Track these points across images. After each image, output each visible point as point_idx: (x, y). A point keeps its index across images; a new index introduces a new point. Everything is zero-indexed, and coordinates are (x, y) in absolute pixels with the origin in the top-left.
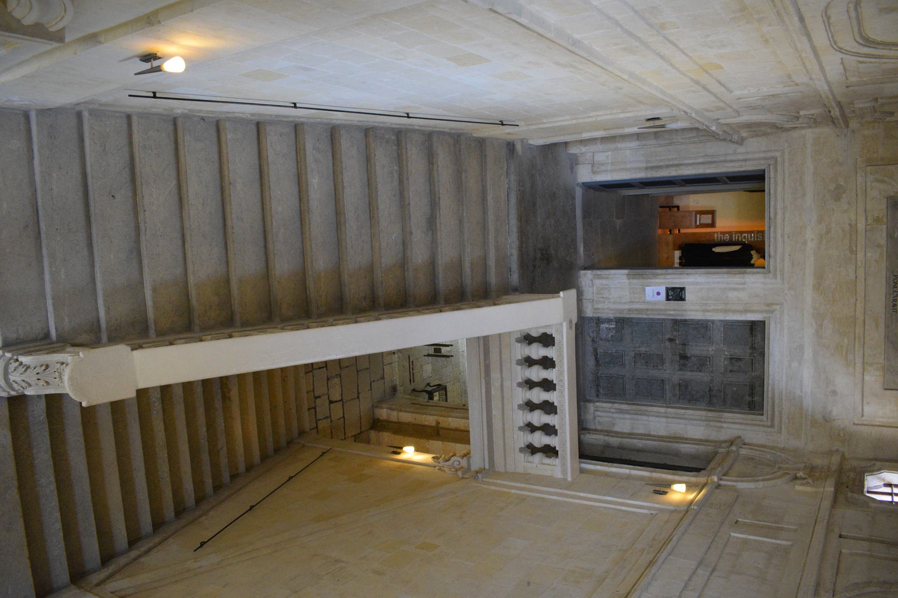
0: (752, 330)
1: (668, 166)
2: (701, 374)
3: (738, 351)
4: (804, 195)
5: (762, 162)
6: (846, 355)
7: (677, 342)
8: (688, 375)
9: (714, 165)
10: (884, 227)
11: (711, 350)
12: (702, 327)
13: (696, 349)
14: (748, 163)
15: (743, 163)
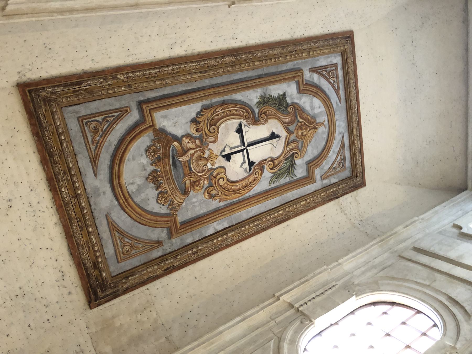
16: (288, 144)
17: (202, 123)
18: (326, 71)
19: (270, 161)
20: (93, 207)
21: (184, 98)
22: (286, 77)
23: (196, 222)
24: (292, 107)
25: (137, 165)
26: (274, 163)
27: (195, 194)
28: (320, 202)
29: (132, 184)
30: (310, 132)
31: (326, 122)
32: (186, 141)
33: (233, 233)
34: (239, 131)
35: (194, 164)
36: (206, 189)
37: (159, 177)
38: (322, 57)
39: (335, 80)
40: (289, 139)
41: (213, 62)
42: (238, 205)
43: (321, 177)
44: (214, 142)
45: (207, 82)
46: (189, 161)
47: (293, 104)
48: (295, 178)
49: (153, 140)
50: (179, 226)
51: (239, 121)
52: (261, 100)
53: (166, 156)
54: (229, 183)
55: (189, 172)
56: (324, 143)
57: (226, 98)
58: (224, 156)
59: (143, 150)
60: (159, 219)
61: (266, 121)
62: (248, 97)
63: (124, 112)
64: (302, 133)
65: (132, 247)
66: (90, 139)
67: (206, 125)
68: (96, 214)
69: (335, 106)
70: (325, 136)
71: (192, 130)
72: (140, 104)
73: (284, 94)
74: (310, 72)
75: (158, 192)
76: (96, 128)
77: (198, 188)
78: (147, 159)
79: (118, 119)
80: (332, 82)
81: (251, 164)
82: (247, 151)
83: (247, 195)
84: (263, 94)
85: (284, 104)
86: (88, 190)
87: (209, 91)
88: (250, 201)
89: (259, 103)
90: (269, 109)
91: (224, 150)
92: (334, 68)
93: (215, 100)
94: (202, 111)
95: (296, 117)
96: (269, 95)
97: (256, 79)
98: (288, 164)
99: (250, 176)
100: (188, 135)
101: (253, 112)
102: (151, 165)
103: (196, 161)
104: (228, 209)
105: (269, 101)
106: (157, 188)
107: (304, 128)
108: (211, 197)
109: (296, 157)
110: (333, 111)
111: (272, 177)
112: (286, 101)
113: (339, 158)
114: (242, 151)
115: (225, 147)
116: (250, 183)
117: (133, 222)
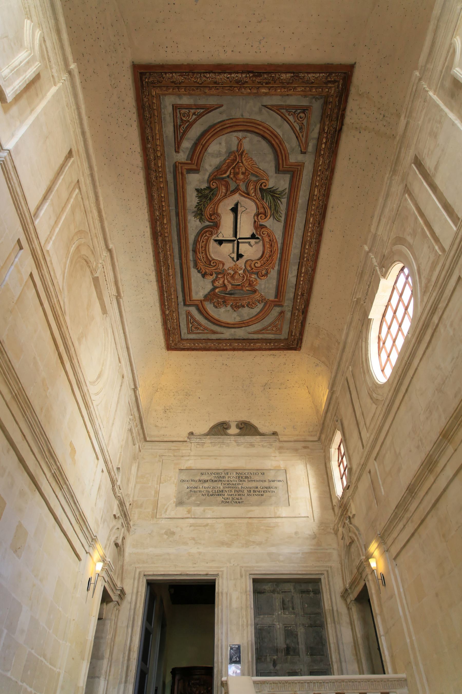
0: (260, 593)
1: (129, 659)
2: (299, 634)
3: (277, 603)
4: (168, 554)
5: (141, 580)
6: (271, 527)
7: (275, 657)
8: (302, 647)
9: (136, 617)
10: (193, 508)
11: (279, 626)
12: (261, 634)
13: (280, 641)
14: (140, 590)
15: (139, 593)
16: (248, 194)
17: (207, 270)
18: (180, 126)
19: (258, 217)
20: (241, 338)
21: (186, 279)
22: (181, 185)
23: (280, 289)
24: (211, 183)
25: (224, 314)
26: (261, 214)
27: (258, 285)
28: (329, 162)
29: (235, 318)
30: (244, 162)
31: (240, 135)
32: (217, 284)
33: (304, 268)
34: (220, 242)
35: (235, 282)
36: (258, 277)
37: (236, 304)
38: (164, 129)
39: (193, 111)
40: (244, 192)
41: (161, 255)
42: (284, 255)
43: (302, 153)
44: (223, 264)
45: (177, 261)
46: (232, 285)
47: (209, 181)
48: (287, 191)
49: (210, 303)
50: (277, 300)
51: (212, 241)
52: (198, 217)
53: (224, 297)
54: (262, 259)
55: (240, 287)
56: (264, 143)
57: (191, 247)
58: (238, 260)
59: (216, 309)
60: (265, 310)
61: (219, 215)
62: (194, 229)
63: (188, 314)
64: (243, 173)
65: (275, 326)
66: (201, 331)
67: (209, 268)
68: (245, 338)
69: (224, 117)
70: (256, 139)
71: (211, 278)
72: (185, 305)
73: (197, 190)
74: (178, 152)
75: (246, 307)
76: (196, 328)
77: (255, 283)
78: (222, 308)
79: (192, 317)
80: (194, 117)
81: (253, 237)
82: (240, 239)
83: (279, 245)
84: (194, 214)
85: (207, 192)
86: (230, 338)
87: (183, 261)
88: (286, 244)
89: (201, 220)
90: (208, 211)
91: (233, 258)
92: (178, 110)
93: (191, 257)
94: (197, 269)
95: (223, 179)
96: (195, 207)
97: (179, 218)
98: (269, 197)
99: (263, 240)
100: (213, 282)
101: (207, 227)
102: (226, 307)
103: (234, 280)
104: (283, 264)
105: (201, 209)
106: (243, 306)
107: (237, 170)
108: (266, 274)
109: (265, 186)
110: (229, 122)
111: (274, 218)
112: (204, 189)
113: (291, 118)
114: (238, 243)
115: (231, 257)
116: (270, 240)
117: (259, 323)
